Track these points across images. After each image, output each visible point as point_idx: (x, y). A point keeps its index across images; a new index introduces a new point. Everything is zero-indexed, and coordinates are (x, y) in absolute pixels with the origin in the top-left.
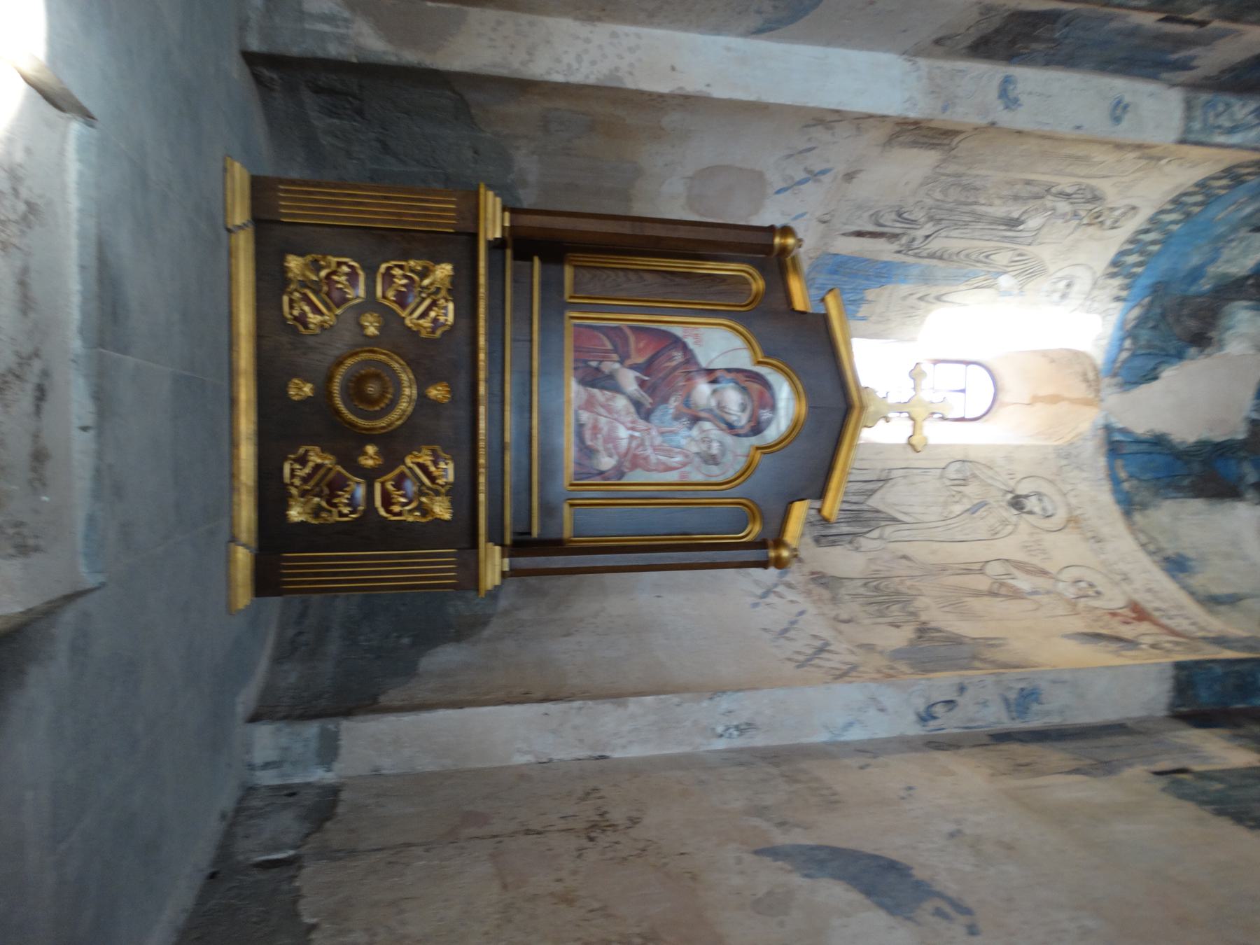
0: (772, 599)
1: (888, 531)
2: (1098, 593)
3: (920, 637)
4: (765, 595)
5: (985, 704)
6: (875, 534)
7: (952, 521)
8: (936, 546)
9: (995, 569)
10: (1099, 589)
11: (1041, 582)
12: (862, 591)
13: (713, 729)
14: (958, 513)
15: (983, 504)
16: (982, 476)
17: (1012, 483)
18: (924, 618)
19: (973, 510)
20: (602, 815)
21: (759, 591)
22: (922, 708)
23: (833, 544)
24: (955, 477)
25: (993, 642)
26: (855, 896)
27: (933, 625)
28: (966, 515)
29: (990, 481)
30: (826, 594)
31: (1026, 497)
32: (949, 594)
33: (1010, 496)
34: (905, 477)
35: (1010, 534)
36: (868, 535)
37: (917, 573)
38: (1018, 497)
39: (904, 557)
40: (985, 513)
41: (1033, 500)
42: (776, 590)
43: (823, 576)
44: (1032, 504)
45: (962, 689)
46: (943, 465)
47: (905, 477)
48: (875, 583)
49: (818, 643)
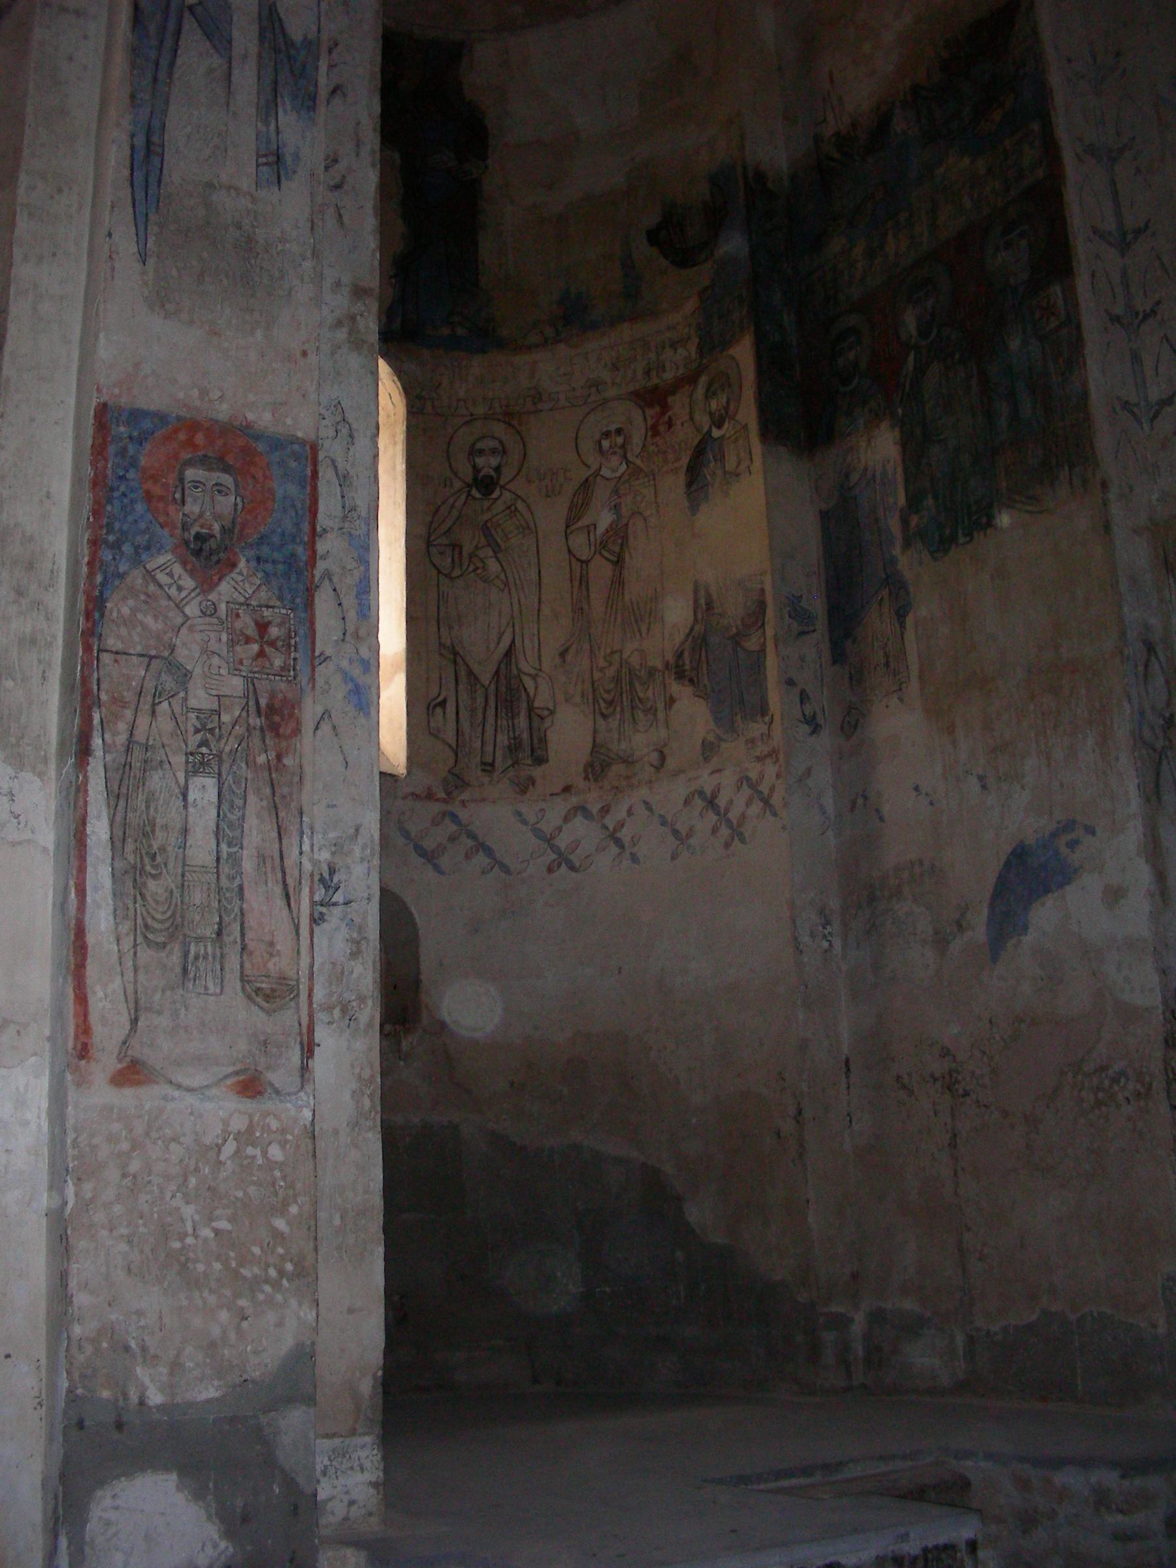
0: (625, 834)
1: (525, 667)
2: (619, 431)
3: (691, 681)
4: (619, 842)
5: (802, 659)
6: (529, 684)
7: (511, 580)
8: (546, 610)
9: (579, 542)
10: (613, 428)
11: (601, 493)
12: (614, 723)
13: (826, 951)
14: (500, 568)
15: (486, 529)
16: (449, 523)
17: (458, 484)
18: (659, 664)
19: (497, 549)
20: (935, 1080)
21: (614, 850)
22: (806, 728)
23: (543, 740)
24: (449, 560)
25: (702, 602)
26: (1050, 901)
27: (670, 657)
28: (500, 555)
29: (455, 513)
30: (617, 769)
31: (476, 470)
32: (619, 619)
33: (474, 492)
34: (450, 627)
35: (529, 507)
36: (532, 694)
37: (586, 646)
38: (475, 479)
39: (563, 654)
40: (500, 533)
41: (480, 461)
42: (611, 828)
43: (590, 765)
44: (488, 463)
45: (790, 682)
46: (436, 572)
47: (450, 627)
48: (603, 705)
49: (698, 803)
